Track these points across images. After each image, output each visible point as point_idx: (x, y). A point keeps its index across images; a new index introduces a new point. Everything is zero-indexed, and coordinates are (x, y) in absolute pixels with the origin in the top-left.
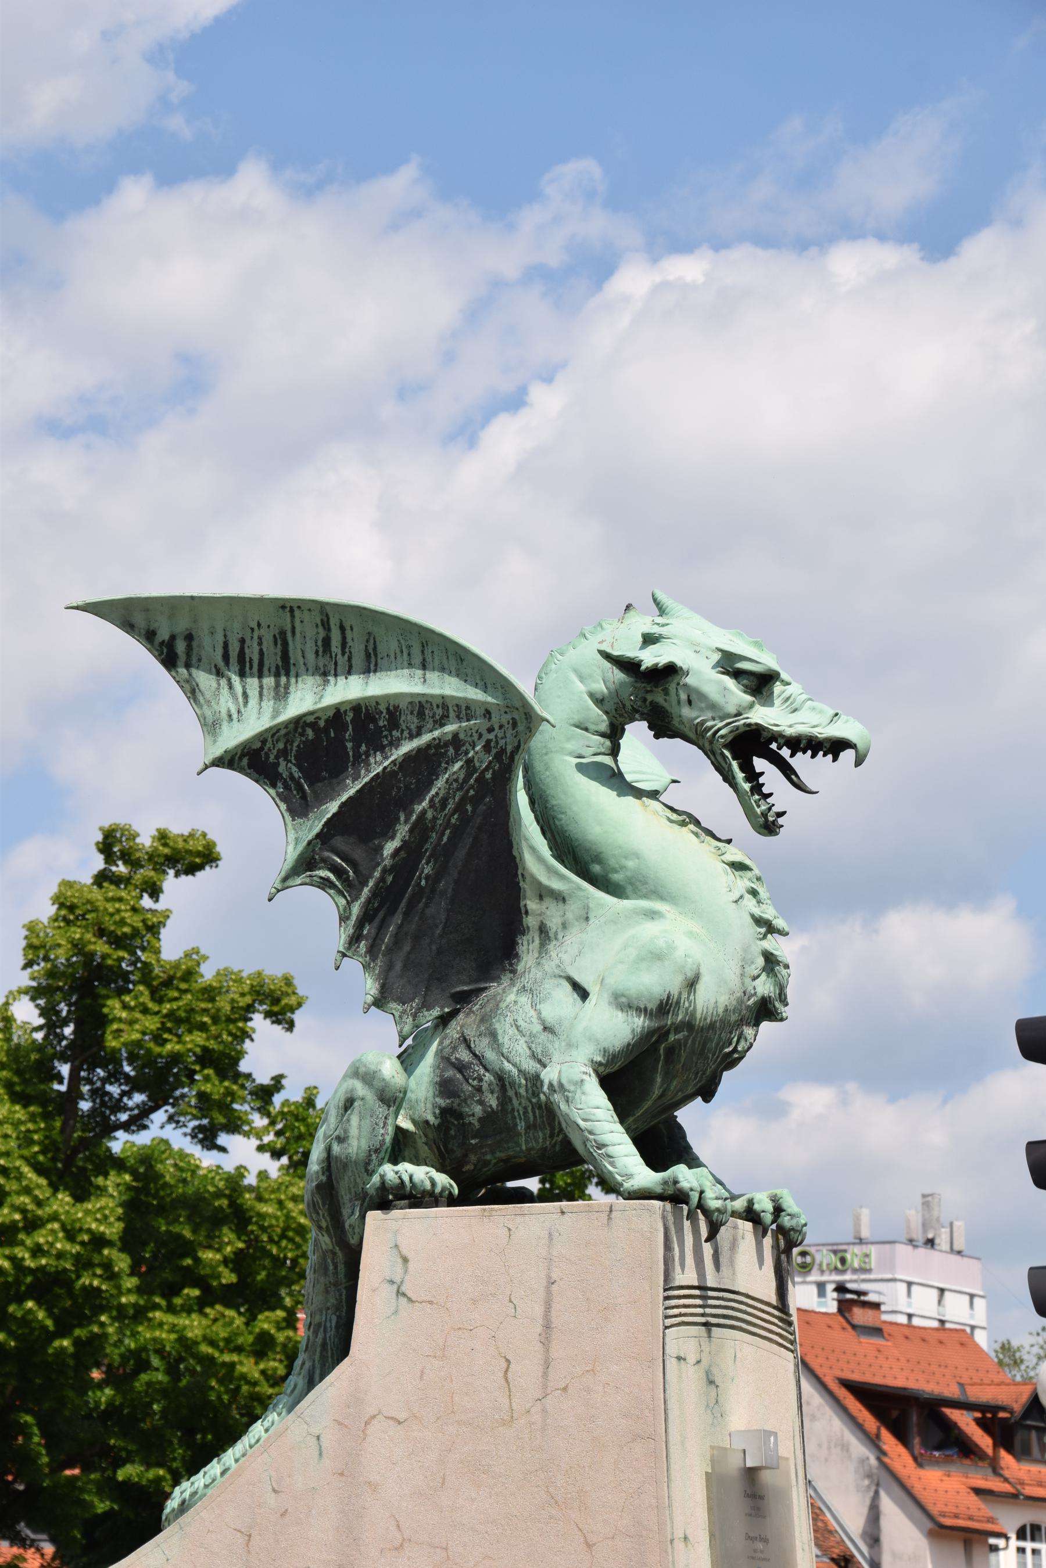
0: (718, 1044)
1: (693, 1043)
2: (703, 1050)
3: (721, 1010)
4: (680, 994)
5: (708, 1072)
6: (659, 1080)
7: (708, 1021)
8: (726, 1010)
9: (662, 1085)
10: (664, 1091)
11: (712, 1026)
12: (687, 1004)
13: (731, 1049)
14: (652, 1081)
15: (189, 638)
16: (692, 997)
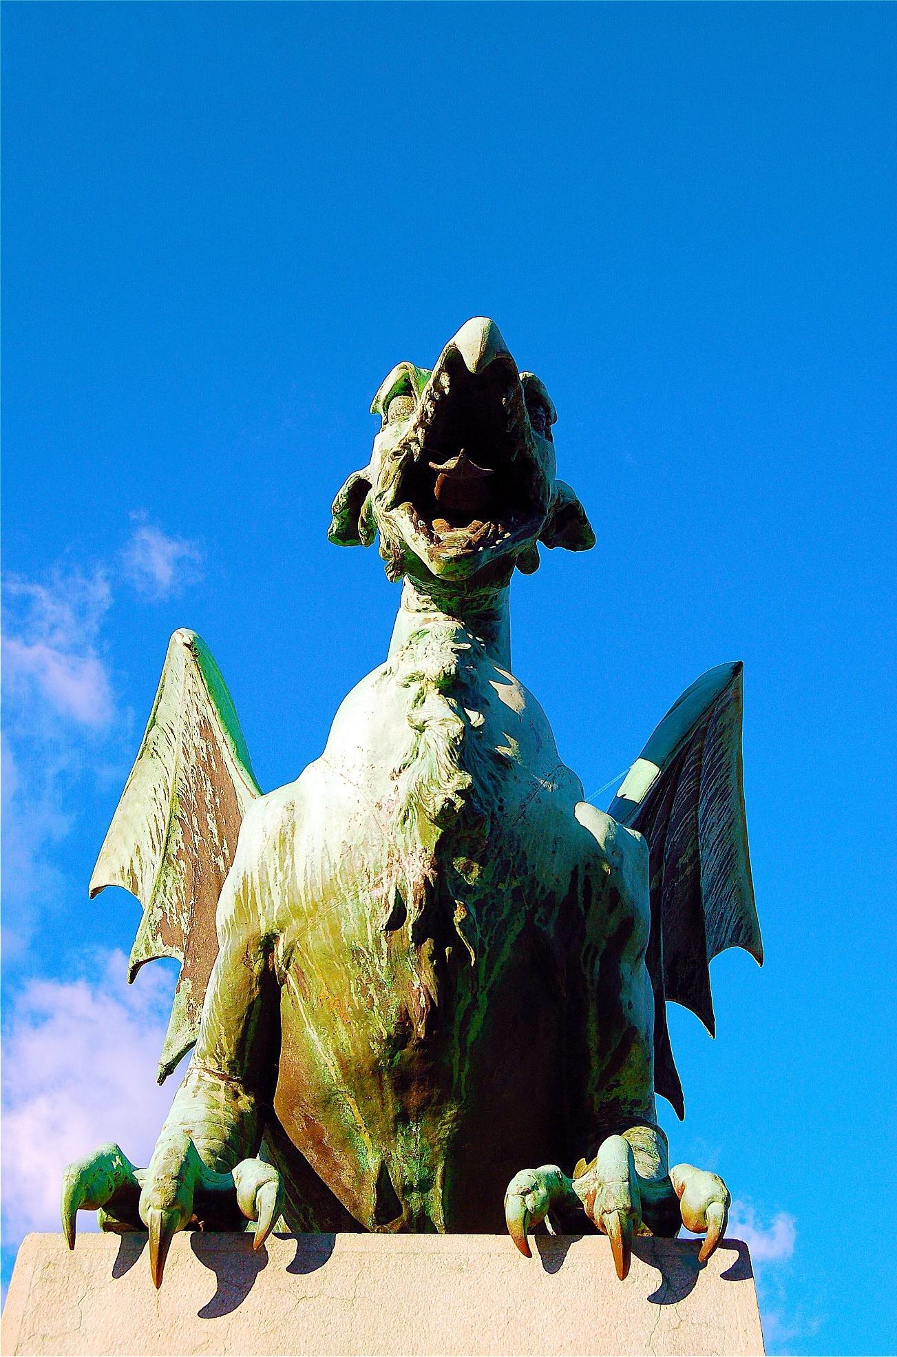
0: (362, 919)
1: (318, 938)
2: (338, 941)
3: (335, 856)
4: (263, 866)
5: (383, 976)
6: (312, 1033)
7: (319, 885)
8: (348, 848)
9: (326, 1044)
10: (337, 1052)
11: (330, 891)
12: (280, 877)
13: (391, 910)
14: (310, 1043)
15: (138, 851)
16: (288, 862)
